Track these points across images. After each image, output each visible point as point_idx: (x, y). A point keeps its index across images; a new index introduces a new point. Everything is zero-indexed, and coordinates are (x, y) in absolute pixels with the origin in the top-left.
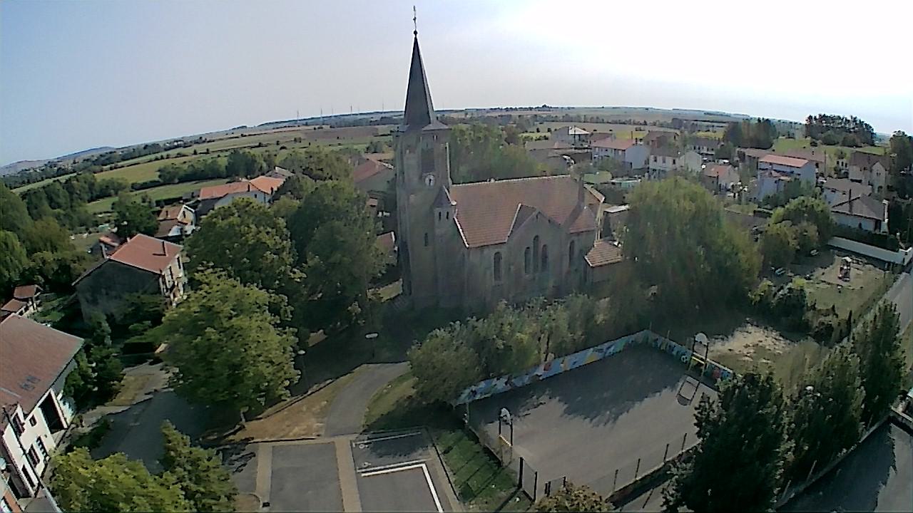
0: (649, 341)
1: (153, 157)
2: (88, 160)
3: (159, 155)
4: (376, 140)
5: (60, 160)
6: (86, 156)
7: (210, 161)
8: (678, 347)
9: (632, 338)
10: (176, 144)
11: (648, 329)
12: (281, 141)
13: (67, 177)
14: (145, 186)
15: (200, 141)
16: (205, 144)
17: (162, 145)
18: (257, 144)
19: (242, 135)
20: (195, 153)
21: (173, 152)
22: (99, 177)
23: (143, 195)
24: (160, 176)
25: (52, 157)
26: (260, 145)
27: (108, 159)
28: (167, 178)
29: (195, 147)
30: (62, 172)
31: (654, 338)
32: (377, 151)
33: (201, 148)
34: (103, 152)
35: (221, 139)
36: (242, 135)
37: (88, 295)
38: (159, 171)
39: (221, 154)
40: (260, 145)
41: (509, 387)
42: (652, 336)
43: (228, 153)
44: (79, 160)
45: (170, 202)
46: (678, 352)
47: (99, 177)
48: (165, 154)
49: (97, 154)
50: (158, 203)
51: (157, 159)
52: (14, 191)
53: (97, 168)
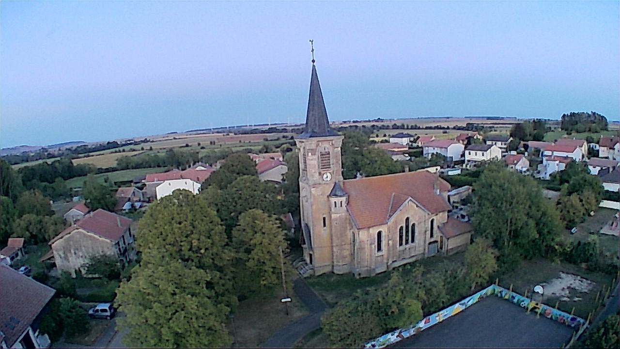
0: (496, 292)
1: (113, 150)
2: (69, 149)
3: (117, 149)
4: (266, 143)
5: (51, 147)
6: (68, 147)
7: (153, 155)
8: (518, 297)
9: (484, 291)
10: (129, 142)
11: (495, 283)
12: (201, 143)
13: (53, 160)
14: (107, 170)
15: (146, 141)
16: (149, 143)
17: (119, 143)
18: (185, 145)
19: (175, 138)
20: (143, 149)
21: (127, 148)
22: (75, 162)
23: (106, 177)
24: (118, 164)
25: (44, 145)
26: (187, 146)
27: (85, 150)
28: (125, 165)
29: (142, 145)
30: (51, 156)
31: (500, 290)
32: (268, 151)
33: (147, 146)
34: (80, 145)
35: (160, 141)
36: (175, 138)
37: (61, 253)
38: (117, 160)
39: (160, 151)
40: (187, 146)
41: (399, 339)
42: (498, 289)
43: (165, 150)
44: (63, 148)
45: (124, 183)
46: (518, 300)
47: (75, 162)
48: (121, 149)
49: (75, 146)
50: (115, 183)
51: (116, 152)
52: (13, 167)
53: (75, 155)
